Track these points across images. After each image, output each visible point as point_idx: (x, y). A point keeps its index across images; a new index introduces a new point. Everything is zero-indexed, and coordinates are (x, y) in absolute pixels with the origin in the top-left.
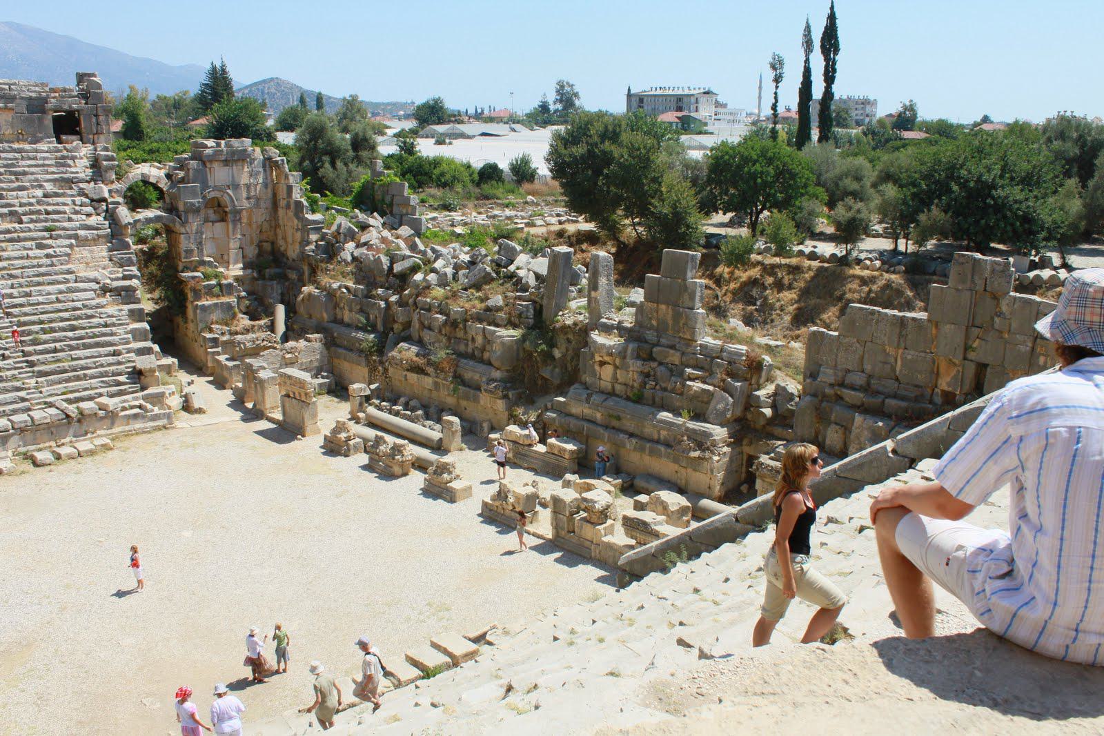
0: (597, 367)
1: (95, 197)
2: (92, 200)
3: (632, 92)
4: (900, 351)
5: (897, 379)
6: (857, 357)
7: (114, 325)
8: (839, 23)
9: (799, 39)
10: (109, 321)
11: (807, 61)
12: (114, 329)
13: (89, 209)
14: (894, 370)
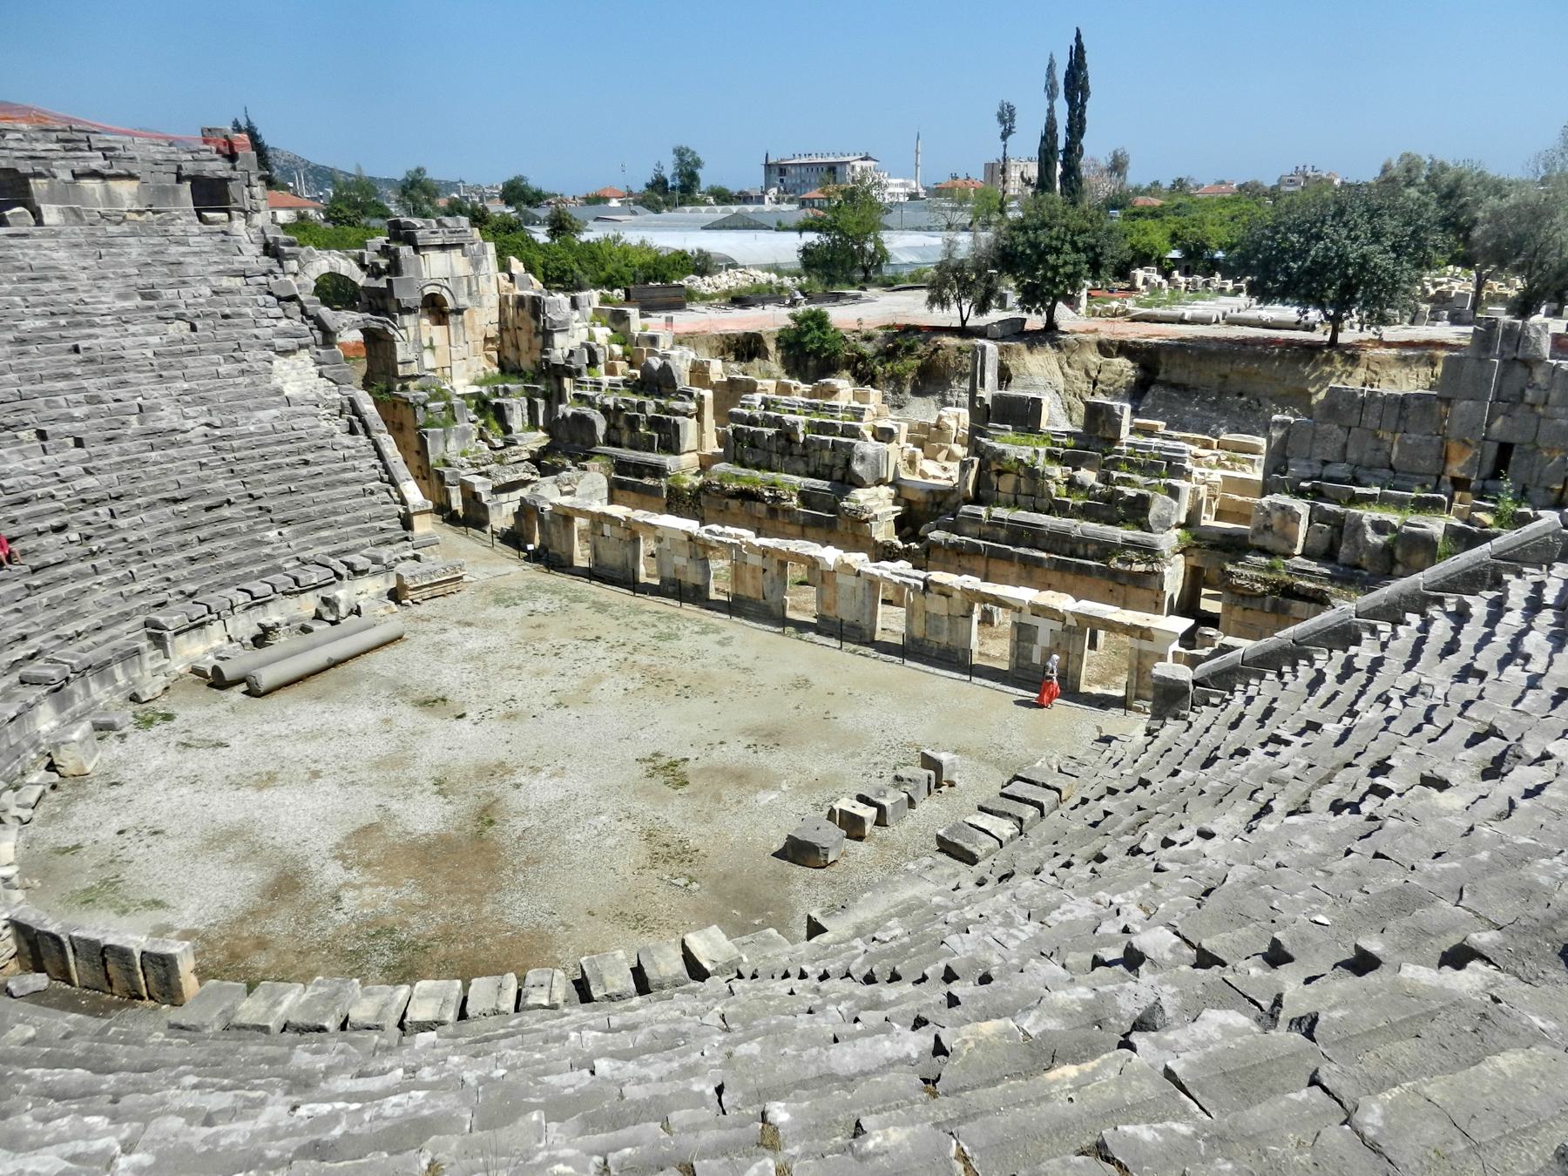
0: (994, 478)
1: (283, 295)
2: (279, 299)
3: (771, 161)
4: (1398, 436)
5: (1391, 468)
6: (1338, 445)
7: (355, 458)
8: (1089, 58)
9: (1042, 80)
10: (347, 453)
11: (1051, 110)
12: (356, 463)
13: (278, 311)
14: (1389, 455)
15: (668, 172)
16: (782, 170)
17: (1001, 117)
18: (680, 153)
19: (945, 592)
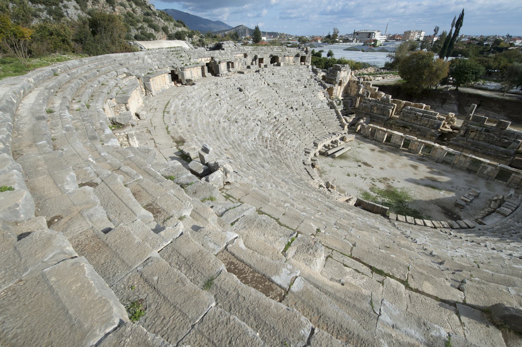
0: (470, 132)
11: (451, 30)
15: (331, 34)
16: (357, 34)
17: (435, 30)
18: (334, 30)
19: (466, 157)
